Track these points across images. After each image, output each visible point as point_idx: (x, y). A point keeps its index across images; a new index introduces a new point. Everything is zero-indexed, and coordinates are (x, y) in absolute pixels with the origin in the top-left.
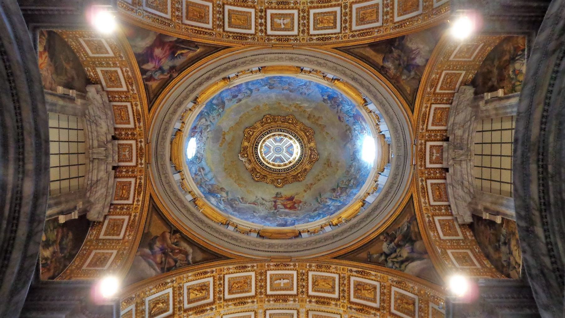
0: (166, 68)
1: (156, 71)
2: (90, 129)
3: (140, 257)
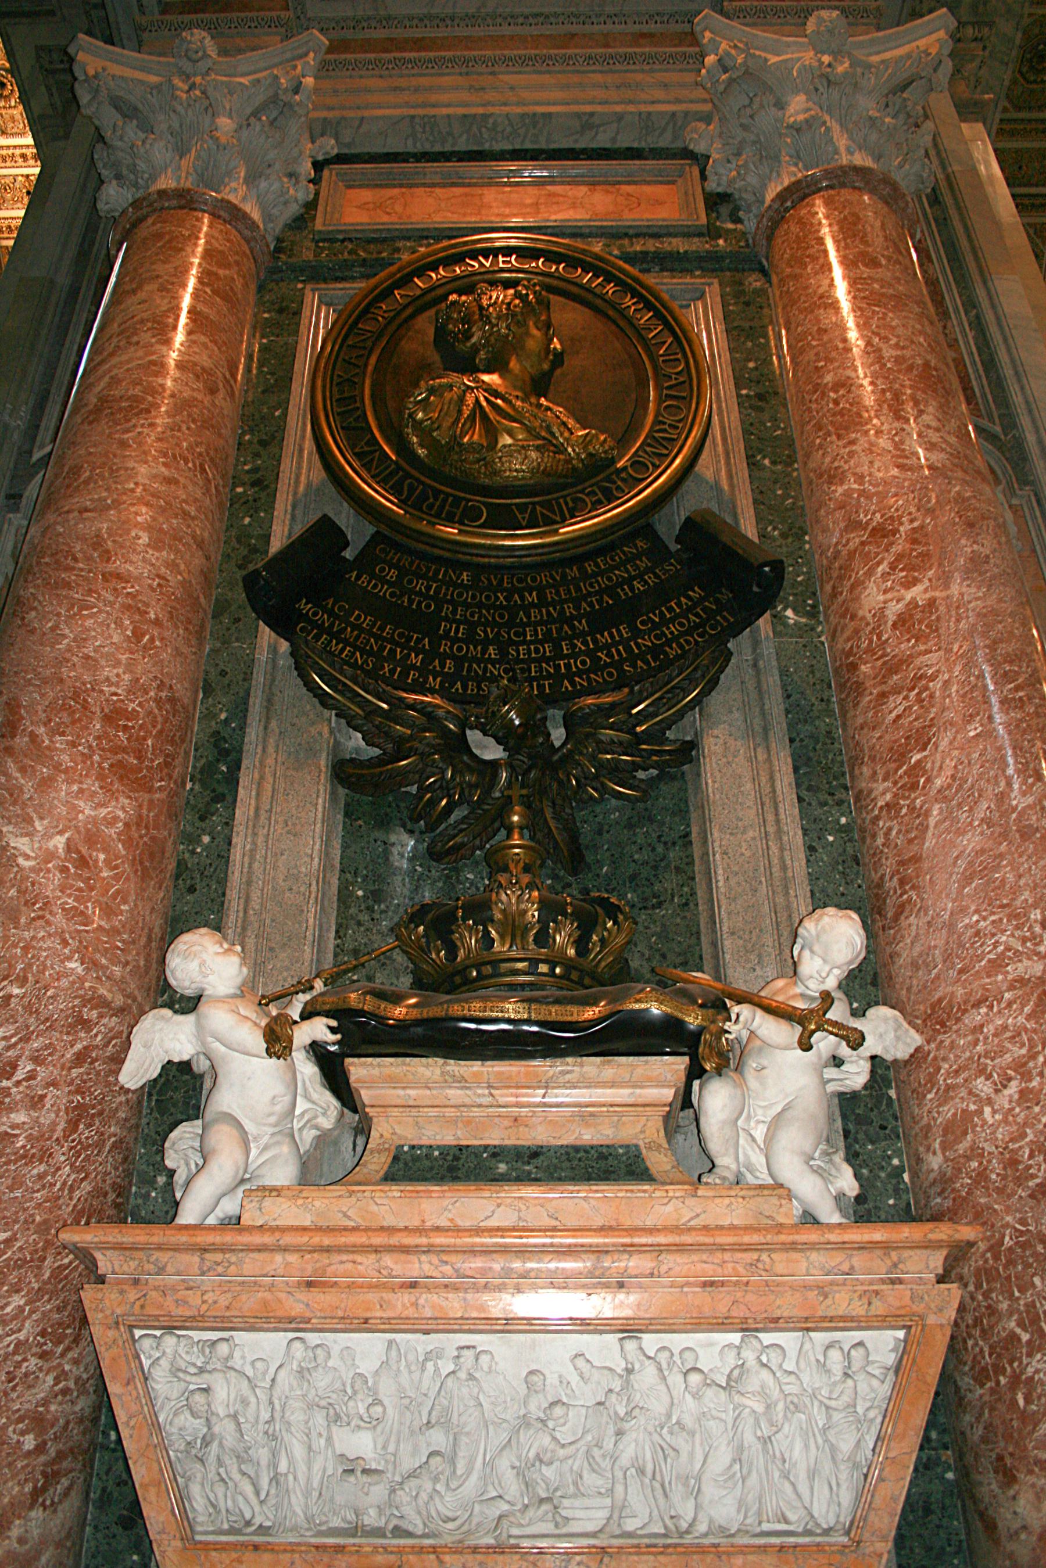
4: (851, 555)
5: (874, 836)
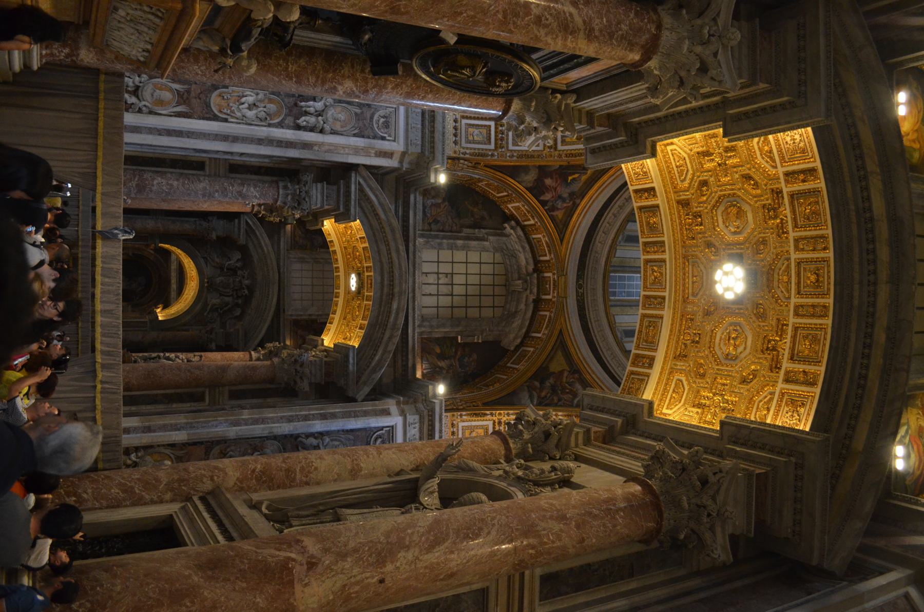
0: (565, 195)
2: (508, 263)
3: (526, 388)
4: (367, 83)
5: (284, 60)
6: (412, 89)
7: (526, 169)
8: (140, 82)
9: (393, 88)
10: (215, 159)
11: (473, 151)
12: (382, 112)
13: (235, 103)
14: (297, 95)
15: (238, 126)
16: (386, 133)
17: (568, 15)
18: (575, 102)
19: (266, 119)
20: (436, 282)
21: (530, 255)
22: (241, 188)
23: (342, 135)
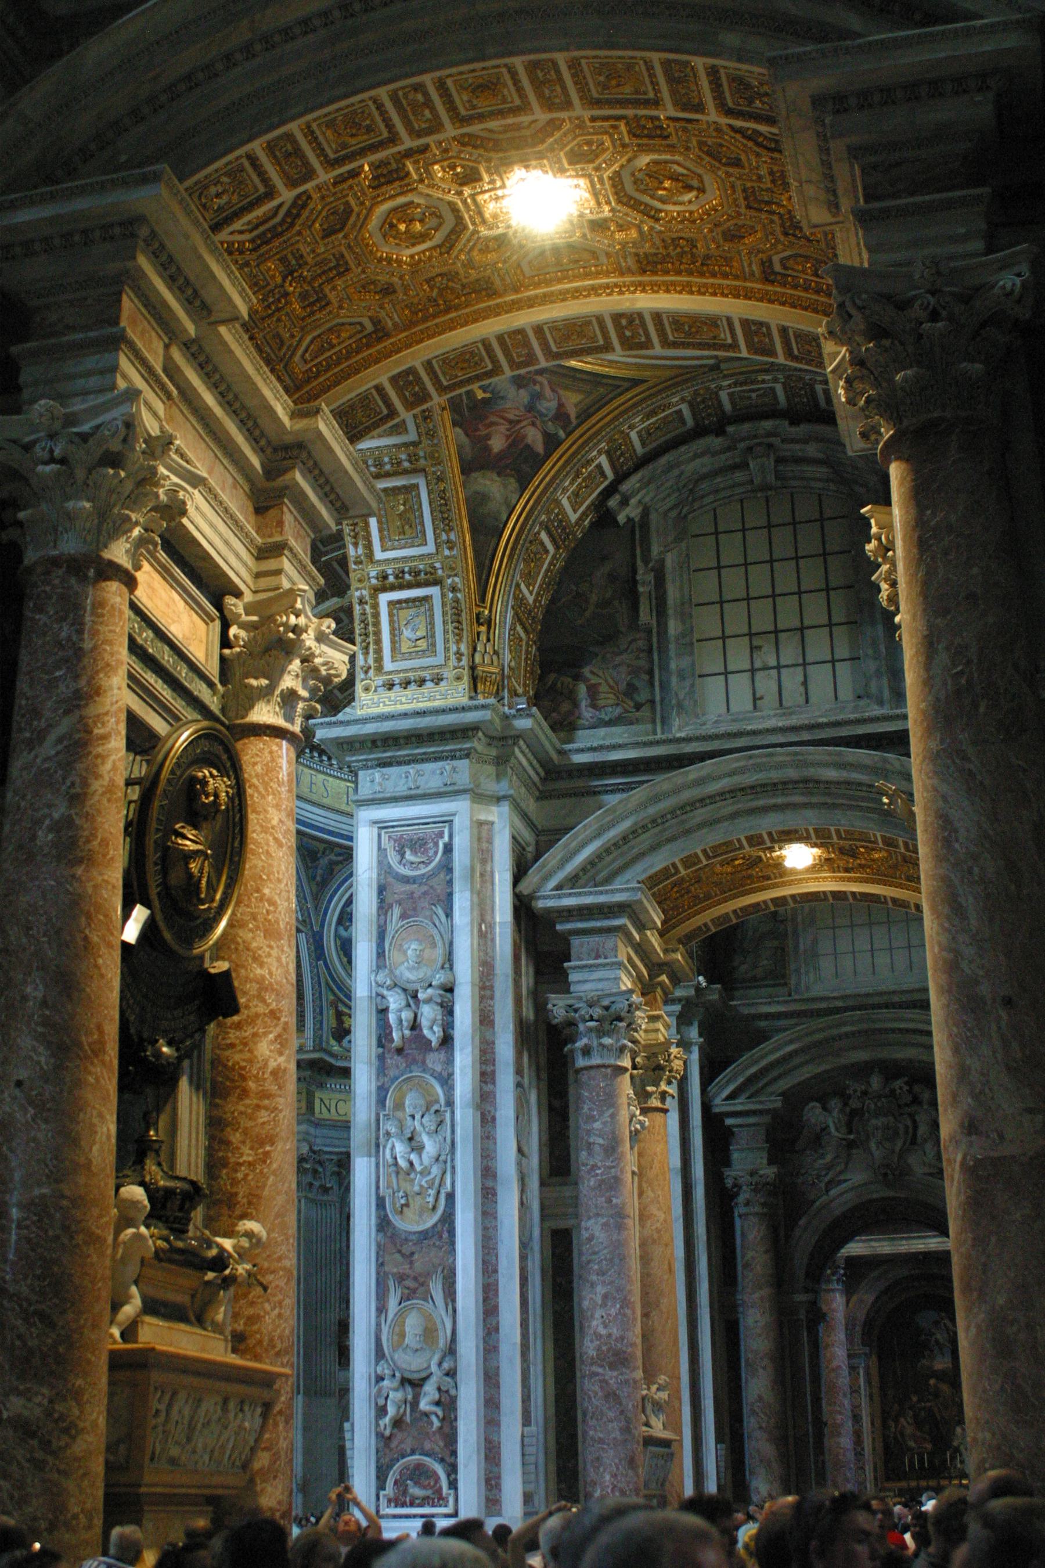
0: (524, 396)
1: (542, 415)
4: (257, 1015)
5: (236, 1171)
6: (258, 928)
7: (476, 503)
8: (394, 1376)
9: (261, 965)
10: (543, 1208)
11: (451, 636)
12: (393, 858)
13: (413, 1181)
14: (381, 1050)
15: (458, 1169)
16: (436, 844)
17: (60, 747)
18: (238, 594)
19: (437, 1111)
20: (774, 672)
21: (683, 449)
22: (597, 1148)
23: (451, 944)
